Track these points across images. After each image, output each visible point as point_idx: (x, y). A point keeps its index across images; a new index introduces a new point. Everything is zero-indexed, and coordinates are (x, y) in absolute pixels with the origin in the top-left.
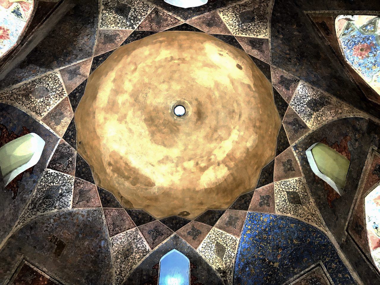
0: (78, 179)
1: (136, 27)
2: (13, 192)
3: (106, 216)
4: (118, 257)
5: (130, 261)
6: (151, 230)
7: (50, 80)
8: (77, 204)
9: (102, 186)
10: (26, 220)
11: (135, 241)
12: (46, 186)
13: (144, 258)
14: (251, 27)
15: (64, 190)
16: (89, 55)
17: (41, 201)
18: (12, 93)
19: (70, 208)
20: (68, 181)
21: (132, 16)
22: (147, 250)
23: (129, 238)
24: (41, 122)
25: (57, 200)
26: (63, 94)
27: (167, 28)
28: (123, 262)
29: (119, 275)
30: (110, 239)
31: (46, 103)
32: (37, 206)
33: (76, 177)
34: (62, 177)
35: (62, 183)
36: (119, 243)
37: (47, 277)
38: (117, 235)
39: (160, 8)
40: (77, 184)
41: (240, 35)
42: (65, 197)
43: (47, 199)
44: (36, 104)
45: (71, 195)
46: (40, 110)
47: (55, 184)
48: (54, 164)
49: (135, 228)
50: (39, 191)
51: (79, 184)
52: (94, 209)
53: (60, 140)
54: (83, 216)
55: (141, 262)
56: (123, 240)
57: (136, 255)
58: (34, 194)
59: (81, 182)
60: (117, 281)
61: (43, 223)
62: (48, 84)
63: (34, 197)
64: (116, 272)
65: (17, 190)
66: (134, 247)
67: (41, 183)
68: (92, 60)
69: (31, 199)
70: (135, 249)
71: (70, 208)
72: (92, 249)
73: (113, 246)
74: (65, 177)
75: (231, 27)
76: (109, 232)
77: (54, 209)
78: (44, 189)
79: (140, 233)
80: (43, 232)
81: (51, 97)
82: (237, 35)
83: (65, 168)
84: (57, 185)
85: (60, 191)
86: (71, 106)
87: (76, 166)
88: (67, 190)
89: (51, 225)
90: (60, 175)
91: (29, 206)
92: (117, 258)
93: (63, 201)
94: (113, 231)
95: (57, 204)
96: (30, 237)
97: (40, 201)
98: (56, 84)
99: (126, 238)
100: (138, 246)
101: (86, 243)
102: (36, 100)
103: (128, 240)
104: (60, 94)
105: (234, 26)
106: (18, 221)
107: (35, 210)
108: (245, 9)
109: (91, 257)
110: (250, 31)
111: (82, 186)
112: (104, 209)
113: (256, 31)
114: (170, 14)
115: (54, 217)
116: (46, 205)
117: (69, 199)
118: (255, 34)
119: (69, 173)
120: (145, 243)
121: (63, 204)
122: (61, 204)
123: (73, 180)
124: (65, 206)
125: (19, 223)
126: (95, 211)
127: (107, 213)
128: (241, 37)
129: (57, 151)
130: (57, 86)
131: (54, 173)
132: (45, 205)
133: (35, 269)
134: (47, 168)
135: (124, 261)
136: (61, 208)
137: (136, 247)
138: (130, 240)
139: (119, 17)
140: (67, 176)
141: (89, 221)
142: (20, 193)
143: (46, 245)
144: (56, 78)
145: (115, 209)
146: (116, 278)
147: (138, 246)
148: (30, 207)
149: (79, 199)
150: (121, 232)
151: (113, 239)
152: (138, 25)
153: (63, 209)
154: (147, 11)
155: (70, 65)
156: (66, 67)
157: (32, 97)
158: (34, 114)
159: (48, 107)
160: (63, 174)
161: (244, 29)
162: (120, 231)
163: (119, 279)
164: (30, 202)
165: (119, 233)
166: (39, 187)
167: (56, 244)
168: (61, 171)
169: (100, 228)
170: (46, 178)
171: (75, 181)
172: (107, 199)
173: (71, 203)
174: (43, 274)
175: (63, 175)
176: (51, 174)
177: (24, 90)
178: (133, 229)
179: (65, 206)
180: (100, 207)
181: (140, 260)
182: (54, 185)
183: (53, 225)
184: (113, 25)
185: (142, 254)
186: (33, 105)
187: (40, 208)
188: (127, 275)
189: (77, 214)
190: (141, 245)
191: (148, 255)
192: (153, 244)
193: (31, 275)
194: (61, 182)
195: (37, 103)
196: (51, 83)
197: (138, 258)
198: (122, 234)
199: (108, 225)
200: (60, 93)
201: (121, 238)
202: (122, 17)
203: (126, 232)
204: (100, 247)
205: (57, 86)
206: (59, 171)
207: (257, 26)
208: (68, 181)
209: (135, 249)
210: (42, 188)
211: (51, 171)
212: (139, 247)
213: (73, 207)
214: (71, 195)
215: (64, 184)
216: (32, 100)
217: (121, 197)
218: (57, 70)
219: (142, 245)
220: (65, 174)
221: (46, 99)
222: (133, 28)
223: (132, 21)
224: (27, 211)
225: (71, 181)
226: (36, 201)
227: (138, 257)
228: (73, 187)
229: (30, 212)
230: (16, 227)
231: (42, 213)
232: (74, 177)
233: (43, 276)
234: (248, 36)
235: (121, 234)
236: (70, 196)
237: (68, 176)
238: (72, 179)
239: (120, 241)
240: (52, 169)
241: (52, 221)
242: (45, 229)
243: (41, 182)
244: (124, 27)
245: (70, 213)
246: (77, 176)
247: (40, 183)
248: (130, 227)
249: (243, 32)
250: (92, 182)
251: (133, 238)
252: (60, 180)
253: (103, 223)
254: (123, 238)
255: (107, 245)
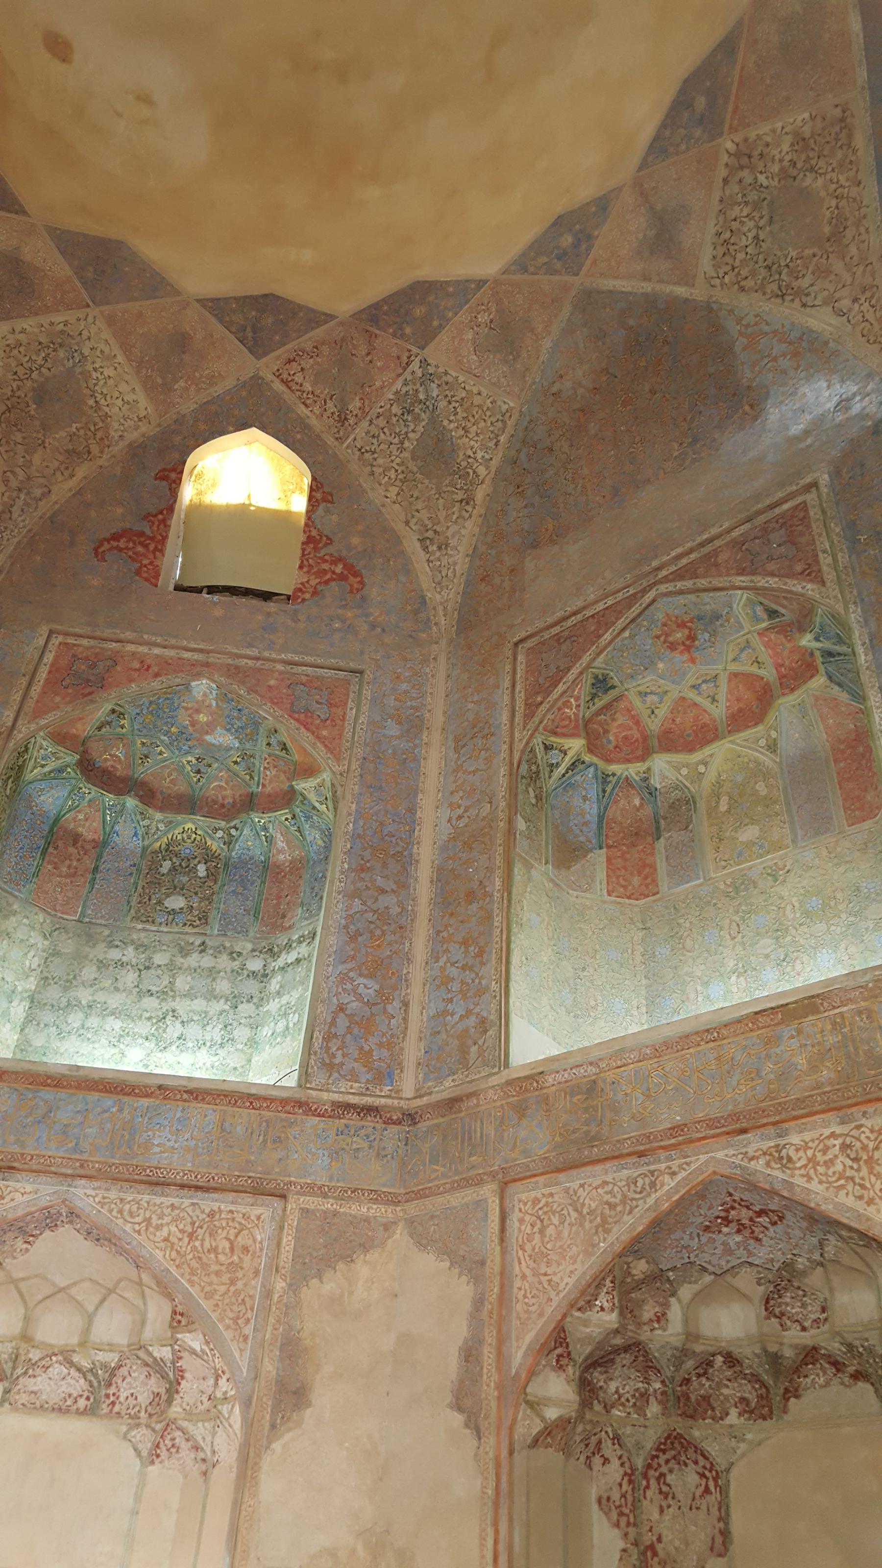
1: (415, 366)
7: (741, 256)
14: (40, 361)
16: (589, 300)
18: (855, 300)
21: (417, 418)
24: (862, 74)
26: (737, 155)
27: (319, 333)
31: (803, 157)
39: (331, 441)
41: (70, 316)
44: (834, 175)
46: (837, 140)
62: (756, 237)
68: (585, 268)
75: (107, 350)
81: (776, 168)
82: (81, 314)
86: (738, 67)
98: (735, 225)
102: (823, 194)
104: (745, 161)
105: (98, 353)
108: (72, 436)
110: (40, 343)
113: (21, 349)
114: (302, 410)
118: (21, 337)
128: (69, 308)
130: (735, 212)
139: (452, 426)
144: (721, 250)
152: (407, 375)
154: (367, 433)
155: (658, 287)
156: (668, 289)
157: (828, 214)
158: (859, 141)
159: (807, 131)
161: (61, 345)
177: (827, 272)
184: (477, 400)
186: (842, 179)
195: (828, 177)
196: (744, 242)
200: (742, 168)
202: (446, 423)
205: (735, 212)
207: (21, 371)
216: (834, 203)
218: (698, 293)
221: (794, 172)
222: (424, 363)
223: (422, 396)
234: (45, 320)
244: (449, 379)
249: (62, 332)
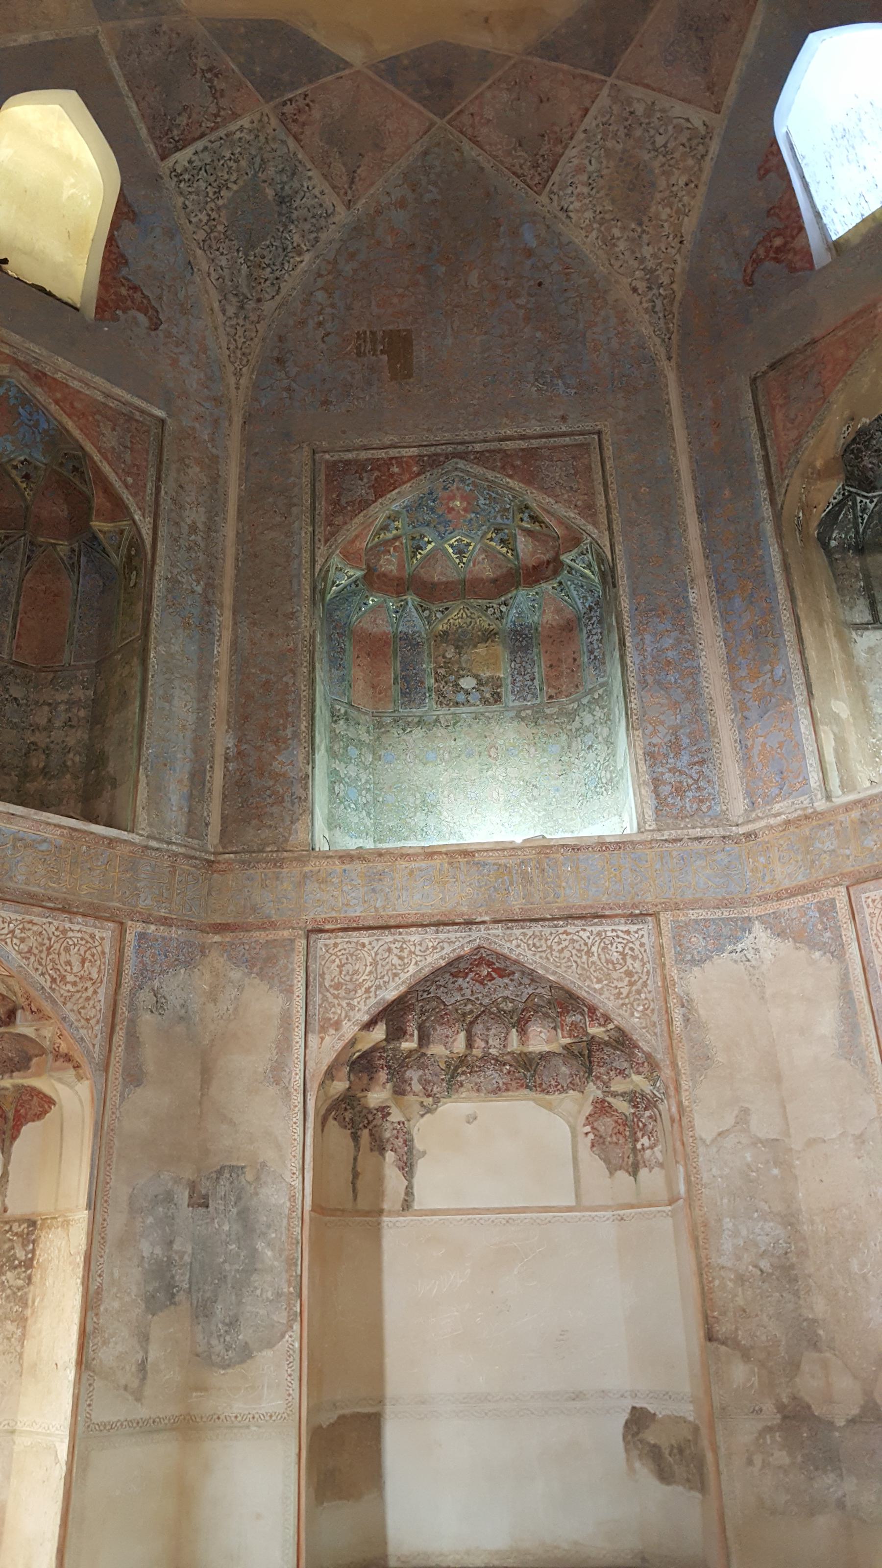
0: (284, 104)
2: (133, 312)
3: (474, 140)
4: (613, 238)
5: (664, 217)
6: (672, 44)
8: (352, 182)
9: (384, 48)
10: (247, 351)
11: (638, 133)
12: (214, 215)
13: (708, 165)
15: (278, 178)
17: (244, 267)
19: (342, 215)
20: (262, 138)
22: (702, 130)
23: (609, 144)
25: (285, 226)
28: (640, 237)
29: (650, 288)
30: (544, 199)
32: (245, 290)
33: (272, 104)
34: (233, 144)
35: (251, 163)
36: (586, 190)
37: (409, 454)
38: (558, 170)
40: (295, 121)
42: (299, 197)
43: (253, 247)
45: (310, 174)
47: (235, 187)
48: (170, 130)
49: (605, 91)
50: (210, 247)
51: (302, 118)
52: (418, 149)
53: (102, 38)
54: (402, 204)
55: (703, 189)
56: (591, 168)
57: (673, 180)
58: (205, 266)
59: (301, 103)
60: (656, 313)
61: (303, 323)
63: (214, 276)
64: (635, 290)
65: (145, 296)
66: (647, 157)
67: (194, 220)
69: (210, 287)
70: (656, 164)
71: (342, 215)
72: (506, 279)
73: (568, 217)
74: (238, 135)
76: (525, 182)
77: (298, 259)
78: (220, 228)
79: (638, 92)
80: (322, 346)
83: (213, 109)
84: (241, 182)
85: (270, 193)
87: (240, 66)
88: (283, 170)
89: (328, 310)
90: (218, 144)
91: (224, 311)
92: (609, 242)
93: (303, 212)
94: (535, 166)
95: (297, 238)
96: (294, 385)
97: (239, 271)
99: (596, 154)
100: (660, 140)
101: (474, 278)
103: (608, 153)
106: (230, 368)
107: (251, 305)
109: (519, 306)
111: (316, 114)
112: (449, 123)
115: (320, 282)
116: (268, 265)
117: (316, 192)
119: (239, 112)
120: (678, 109)
121: (314, 220)
122: (307, 226)
123: (274, 122)
124: (323, 222)
125: (238, 374)
126: (426, 153)
127: (473, 126)
129: (130, 79)
131: (196, 153)
132: (264, 268)
133: (363, 455)
134: (163, 158)
135: (644, 231)
136: (317, 239)
137: (653, 154)
138: (619, 147)
140: (241, 129)
141: (434, 202)
142: (160, 298)
143: (352, 374)
145: (489, 87)
146: (645, 305)
147: (660, 140)
148: (231, 311)
149: (345, 164)
150: (566, 147)
151: (552, 192)
153: (323, 236)
160: (222, 132)
162: (559, 149)
163: (658, 302)
164: (215, 296)
165: (561, 156)
166: (201, 235)
167: (382, 352)
168: (212, 129)
169: (488, 194)
170: (190, 193)
171: (283, 119)
172: (435, 76)
173: (330, 199)
174: (393, 453)
175: (227, 135)
176: (194, 170)
178: (604, 99)
179: (323, 222)
180: (432, 124)
181: (696, 186)
182: (236, 192)
183: (333, 306)
185: (690, 162)
187: (259, 288)
188: (678, 270)
189: (379, 212)
190: (666, 130)
191: (714, 147)
192: (710, 88)
193: (361, 479)
194: (243, 163)
197: (687, 185)
198: (574, 152)
199: (502, 162)
201: (581, 169)
203: (585, 131)
204: (529, 253)
206: (203, 135)
208: (262, 138)
209: (656, 164)
210: (212, 231)
211: (182, 157)
212: (665, 146)
213: (349, 205)
214: (310, 174)
215: (258, 160)
217: (486, 20)
219: (670, 128)
220: (233, 127)
224: (231, 326)
225: (270, 131)
226: (232, 281)
227: (681, 183)
228: (291, 142)
229: (241, 322)
230: (237, 388)
231: (278, 298)
232: (267, 108)
233: (396, 458)
235: (571, 153)
236: (310, 178)
237: (245, 122)
238: (265, 119)
239: (584, 178)
240: (177, 149)
241: (320, 296)
242: (321, 332)
243: (188, 217)
245: (356, 230)
246: (272, 98)
247: (190, 222)
248: (587, 103)
250: (338, 69)
251: (622, 132)
252: (237, 161)
253: (482, 169)
254: (586, 162)
255: (548, 227)
